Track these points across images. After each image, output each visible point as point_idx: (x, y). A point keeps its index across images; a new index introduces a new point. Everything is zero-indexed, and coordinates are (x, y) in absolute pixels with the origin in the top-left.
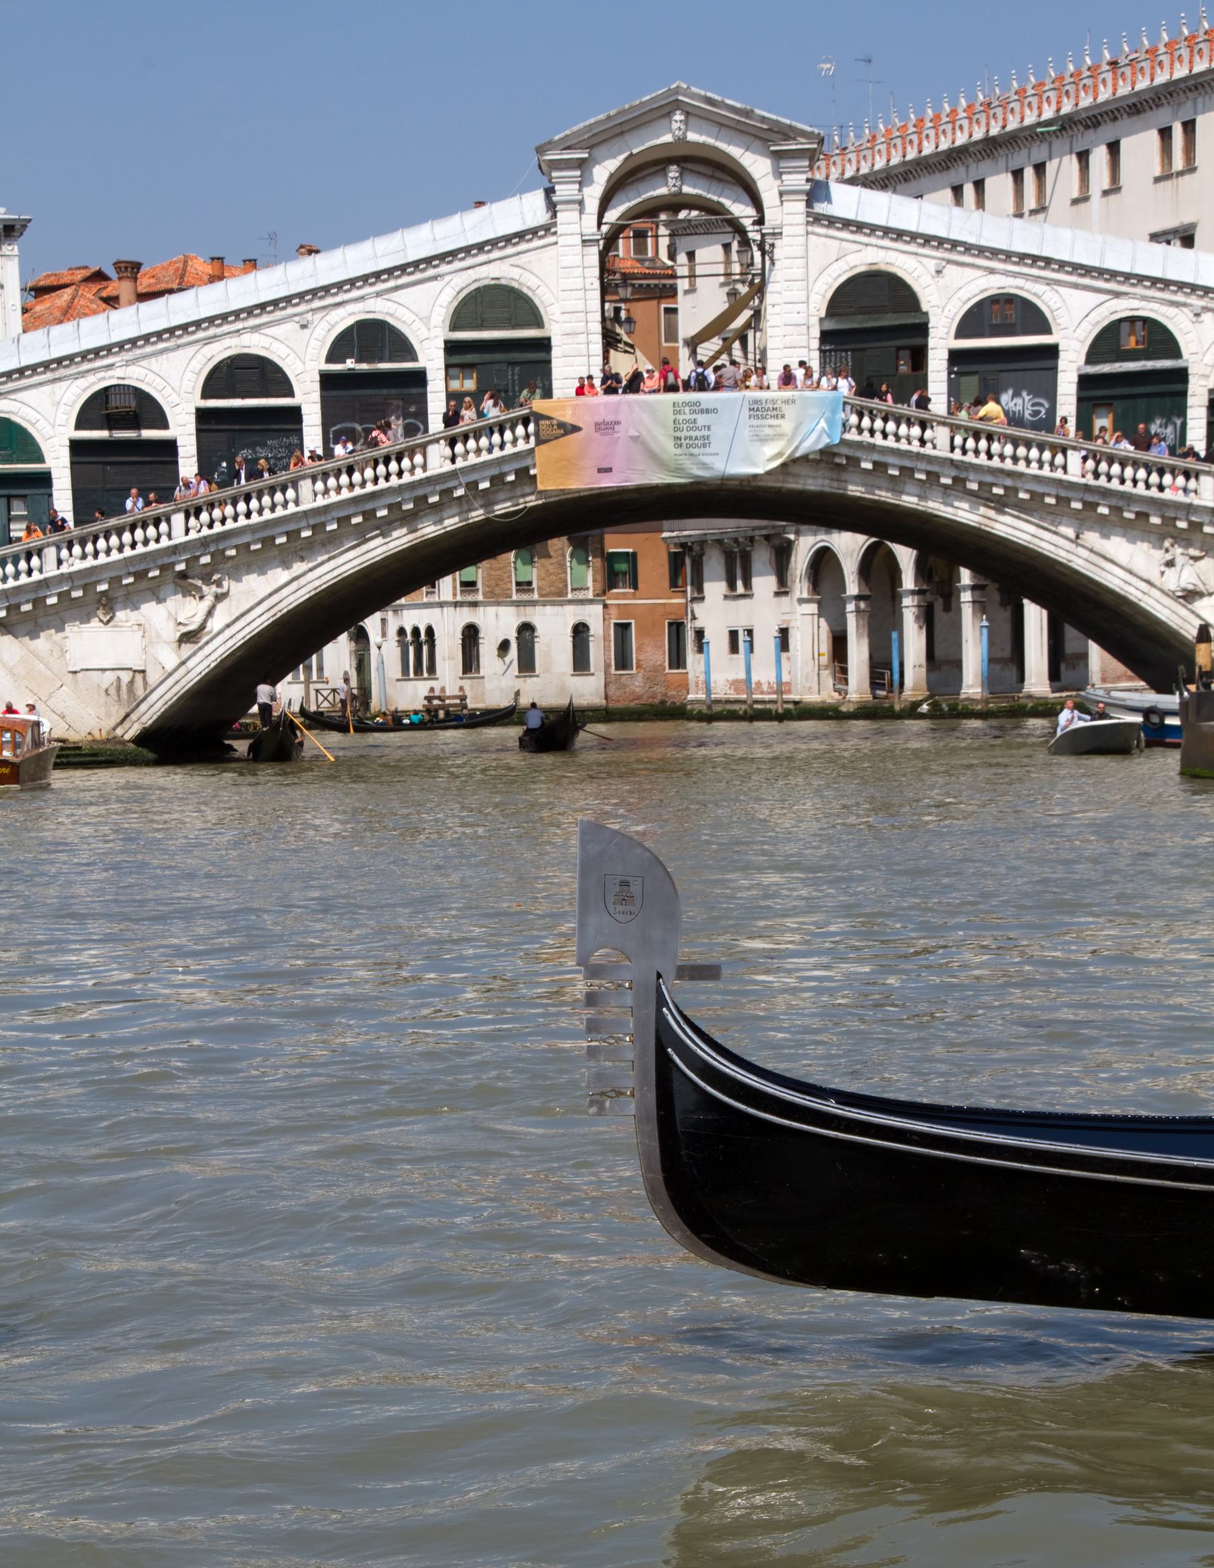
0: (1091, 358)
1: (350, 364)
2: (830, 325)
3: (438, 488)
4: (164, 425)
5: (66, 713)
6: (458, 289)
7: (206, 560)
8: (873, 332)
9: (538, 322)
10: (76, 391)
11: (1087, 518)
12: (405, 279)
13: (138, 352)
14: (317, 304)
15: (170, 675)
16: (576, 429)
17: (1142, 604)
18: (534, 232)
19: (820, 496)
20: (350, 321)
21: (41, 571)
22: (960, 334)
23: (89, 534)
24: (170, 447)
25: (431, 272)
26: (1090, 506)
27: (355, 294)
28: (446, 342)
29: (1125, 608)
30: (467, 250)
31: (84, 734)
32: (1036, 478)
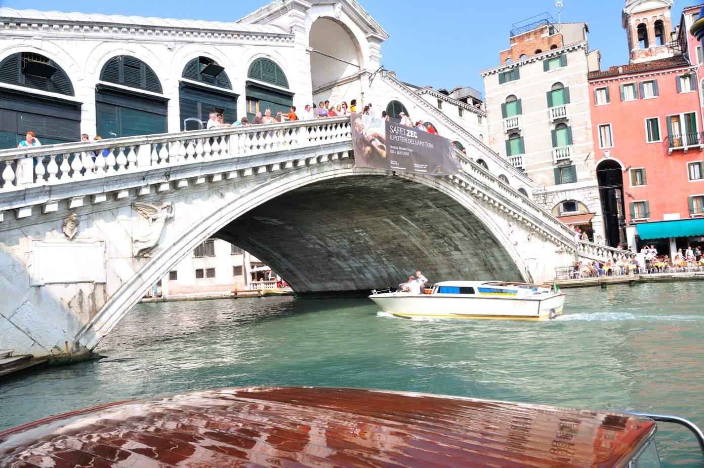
3: (307, 156)
4: (71, 92)
5: (31, 328)
6: (252, 56)
12: (226, 40)
13: (52, 32)
14: (178, 38)
15: (129, 286)
17: (506, 248)
20: (197, 55)
21: (14, 183)
23: (67, 151)
24: (76, 107)
25: (238, 41)
27: (199, 39)
28: (247, 82)
31: (49, 350)
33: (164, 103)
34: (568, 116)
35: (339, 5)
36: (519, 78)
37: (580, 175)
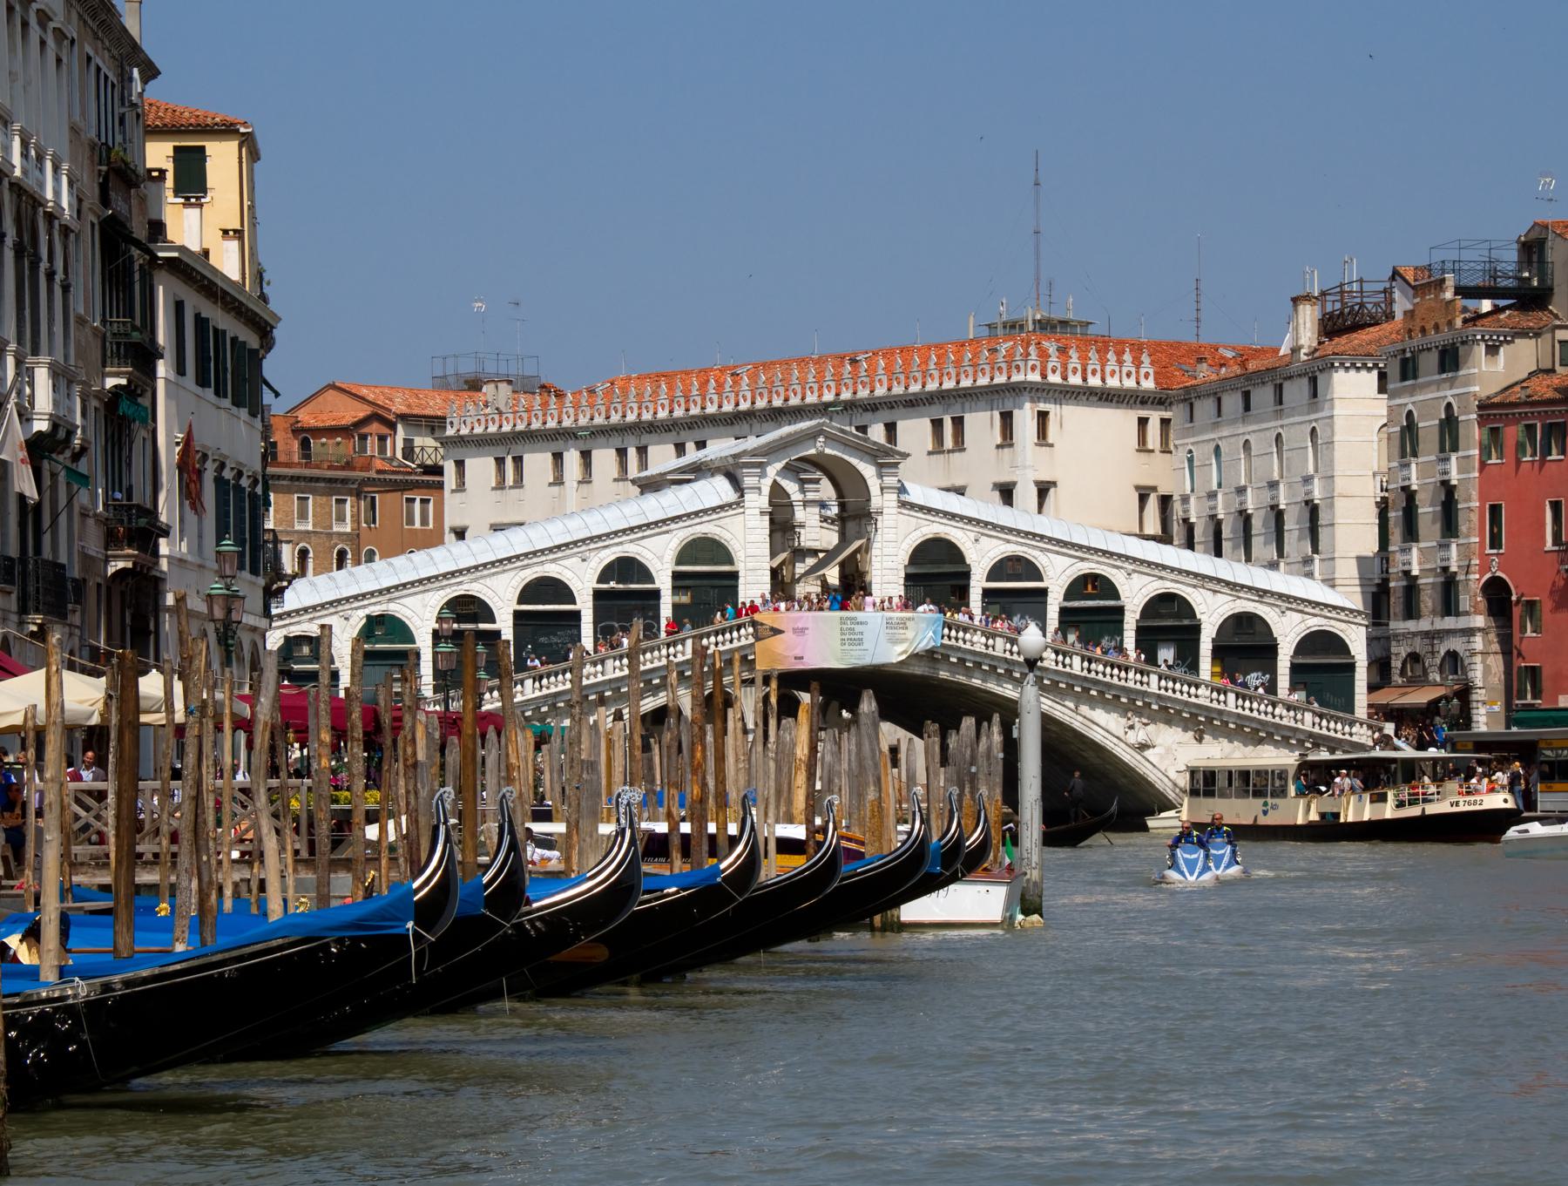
0: (1069, 595)
1: (612, 584)
2: (912, 570)
4: (493, 621)
7: (544, 709)
8: (937, 575)
9: (731, 562)
10: (436, 599)
11: (1084, 697)
14: (592, 546)
16: (781, 632)
18: (730, 505)
19: (922, 677)
20: (613, 557)
22: (988, 580)
25: (665, 528)
26: (1086, 690)
27: (617, 540)
29: (1089, 755)
30: (688, 515)
32: (1056, 672)
33: (576, 615)
34: (1454, 478)
35: (821, 439)
36: (1415, 377)
37: (1465, 602)
